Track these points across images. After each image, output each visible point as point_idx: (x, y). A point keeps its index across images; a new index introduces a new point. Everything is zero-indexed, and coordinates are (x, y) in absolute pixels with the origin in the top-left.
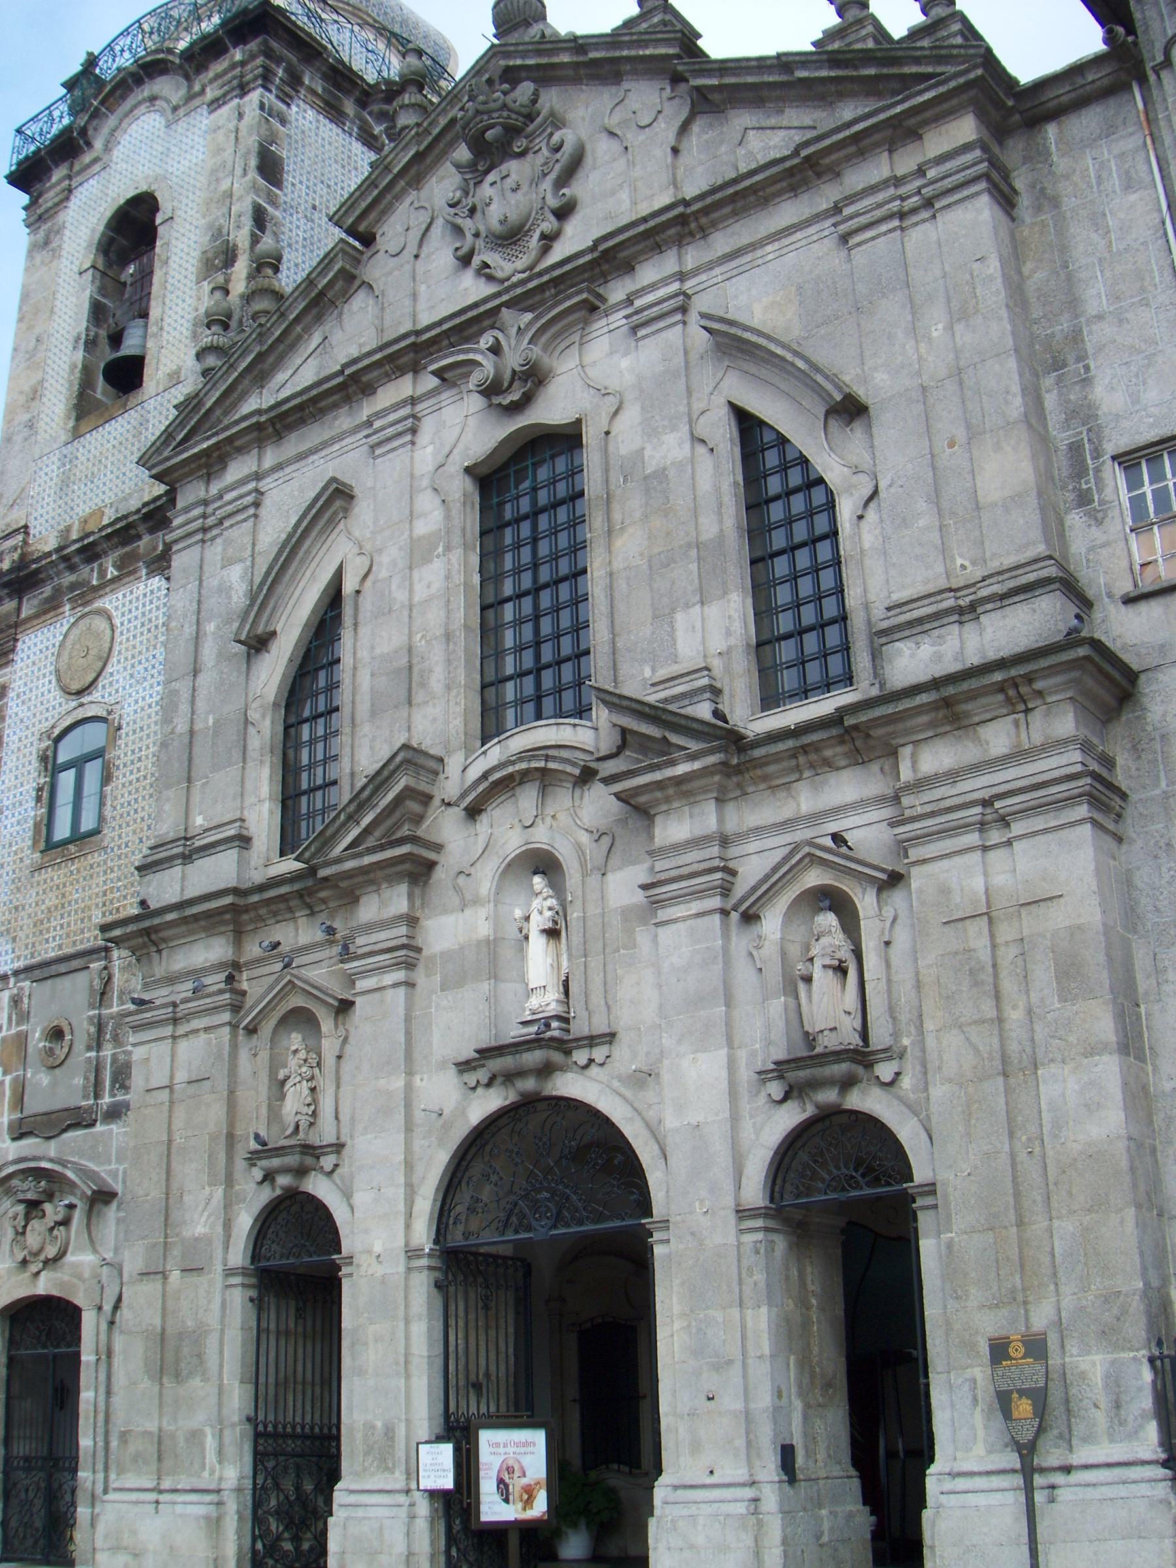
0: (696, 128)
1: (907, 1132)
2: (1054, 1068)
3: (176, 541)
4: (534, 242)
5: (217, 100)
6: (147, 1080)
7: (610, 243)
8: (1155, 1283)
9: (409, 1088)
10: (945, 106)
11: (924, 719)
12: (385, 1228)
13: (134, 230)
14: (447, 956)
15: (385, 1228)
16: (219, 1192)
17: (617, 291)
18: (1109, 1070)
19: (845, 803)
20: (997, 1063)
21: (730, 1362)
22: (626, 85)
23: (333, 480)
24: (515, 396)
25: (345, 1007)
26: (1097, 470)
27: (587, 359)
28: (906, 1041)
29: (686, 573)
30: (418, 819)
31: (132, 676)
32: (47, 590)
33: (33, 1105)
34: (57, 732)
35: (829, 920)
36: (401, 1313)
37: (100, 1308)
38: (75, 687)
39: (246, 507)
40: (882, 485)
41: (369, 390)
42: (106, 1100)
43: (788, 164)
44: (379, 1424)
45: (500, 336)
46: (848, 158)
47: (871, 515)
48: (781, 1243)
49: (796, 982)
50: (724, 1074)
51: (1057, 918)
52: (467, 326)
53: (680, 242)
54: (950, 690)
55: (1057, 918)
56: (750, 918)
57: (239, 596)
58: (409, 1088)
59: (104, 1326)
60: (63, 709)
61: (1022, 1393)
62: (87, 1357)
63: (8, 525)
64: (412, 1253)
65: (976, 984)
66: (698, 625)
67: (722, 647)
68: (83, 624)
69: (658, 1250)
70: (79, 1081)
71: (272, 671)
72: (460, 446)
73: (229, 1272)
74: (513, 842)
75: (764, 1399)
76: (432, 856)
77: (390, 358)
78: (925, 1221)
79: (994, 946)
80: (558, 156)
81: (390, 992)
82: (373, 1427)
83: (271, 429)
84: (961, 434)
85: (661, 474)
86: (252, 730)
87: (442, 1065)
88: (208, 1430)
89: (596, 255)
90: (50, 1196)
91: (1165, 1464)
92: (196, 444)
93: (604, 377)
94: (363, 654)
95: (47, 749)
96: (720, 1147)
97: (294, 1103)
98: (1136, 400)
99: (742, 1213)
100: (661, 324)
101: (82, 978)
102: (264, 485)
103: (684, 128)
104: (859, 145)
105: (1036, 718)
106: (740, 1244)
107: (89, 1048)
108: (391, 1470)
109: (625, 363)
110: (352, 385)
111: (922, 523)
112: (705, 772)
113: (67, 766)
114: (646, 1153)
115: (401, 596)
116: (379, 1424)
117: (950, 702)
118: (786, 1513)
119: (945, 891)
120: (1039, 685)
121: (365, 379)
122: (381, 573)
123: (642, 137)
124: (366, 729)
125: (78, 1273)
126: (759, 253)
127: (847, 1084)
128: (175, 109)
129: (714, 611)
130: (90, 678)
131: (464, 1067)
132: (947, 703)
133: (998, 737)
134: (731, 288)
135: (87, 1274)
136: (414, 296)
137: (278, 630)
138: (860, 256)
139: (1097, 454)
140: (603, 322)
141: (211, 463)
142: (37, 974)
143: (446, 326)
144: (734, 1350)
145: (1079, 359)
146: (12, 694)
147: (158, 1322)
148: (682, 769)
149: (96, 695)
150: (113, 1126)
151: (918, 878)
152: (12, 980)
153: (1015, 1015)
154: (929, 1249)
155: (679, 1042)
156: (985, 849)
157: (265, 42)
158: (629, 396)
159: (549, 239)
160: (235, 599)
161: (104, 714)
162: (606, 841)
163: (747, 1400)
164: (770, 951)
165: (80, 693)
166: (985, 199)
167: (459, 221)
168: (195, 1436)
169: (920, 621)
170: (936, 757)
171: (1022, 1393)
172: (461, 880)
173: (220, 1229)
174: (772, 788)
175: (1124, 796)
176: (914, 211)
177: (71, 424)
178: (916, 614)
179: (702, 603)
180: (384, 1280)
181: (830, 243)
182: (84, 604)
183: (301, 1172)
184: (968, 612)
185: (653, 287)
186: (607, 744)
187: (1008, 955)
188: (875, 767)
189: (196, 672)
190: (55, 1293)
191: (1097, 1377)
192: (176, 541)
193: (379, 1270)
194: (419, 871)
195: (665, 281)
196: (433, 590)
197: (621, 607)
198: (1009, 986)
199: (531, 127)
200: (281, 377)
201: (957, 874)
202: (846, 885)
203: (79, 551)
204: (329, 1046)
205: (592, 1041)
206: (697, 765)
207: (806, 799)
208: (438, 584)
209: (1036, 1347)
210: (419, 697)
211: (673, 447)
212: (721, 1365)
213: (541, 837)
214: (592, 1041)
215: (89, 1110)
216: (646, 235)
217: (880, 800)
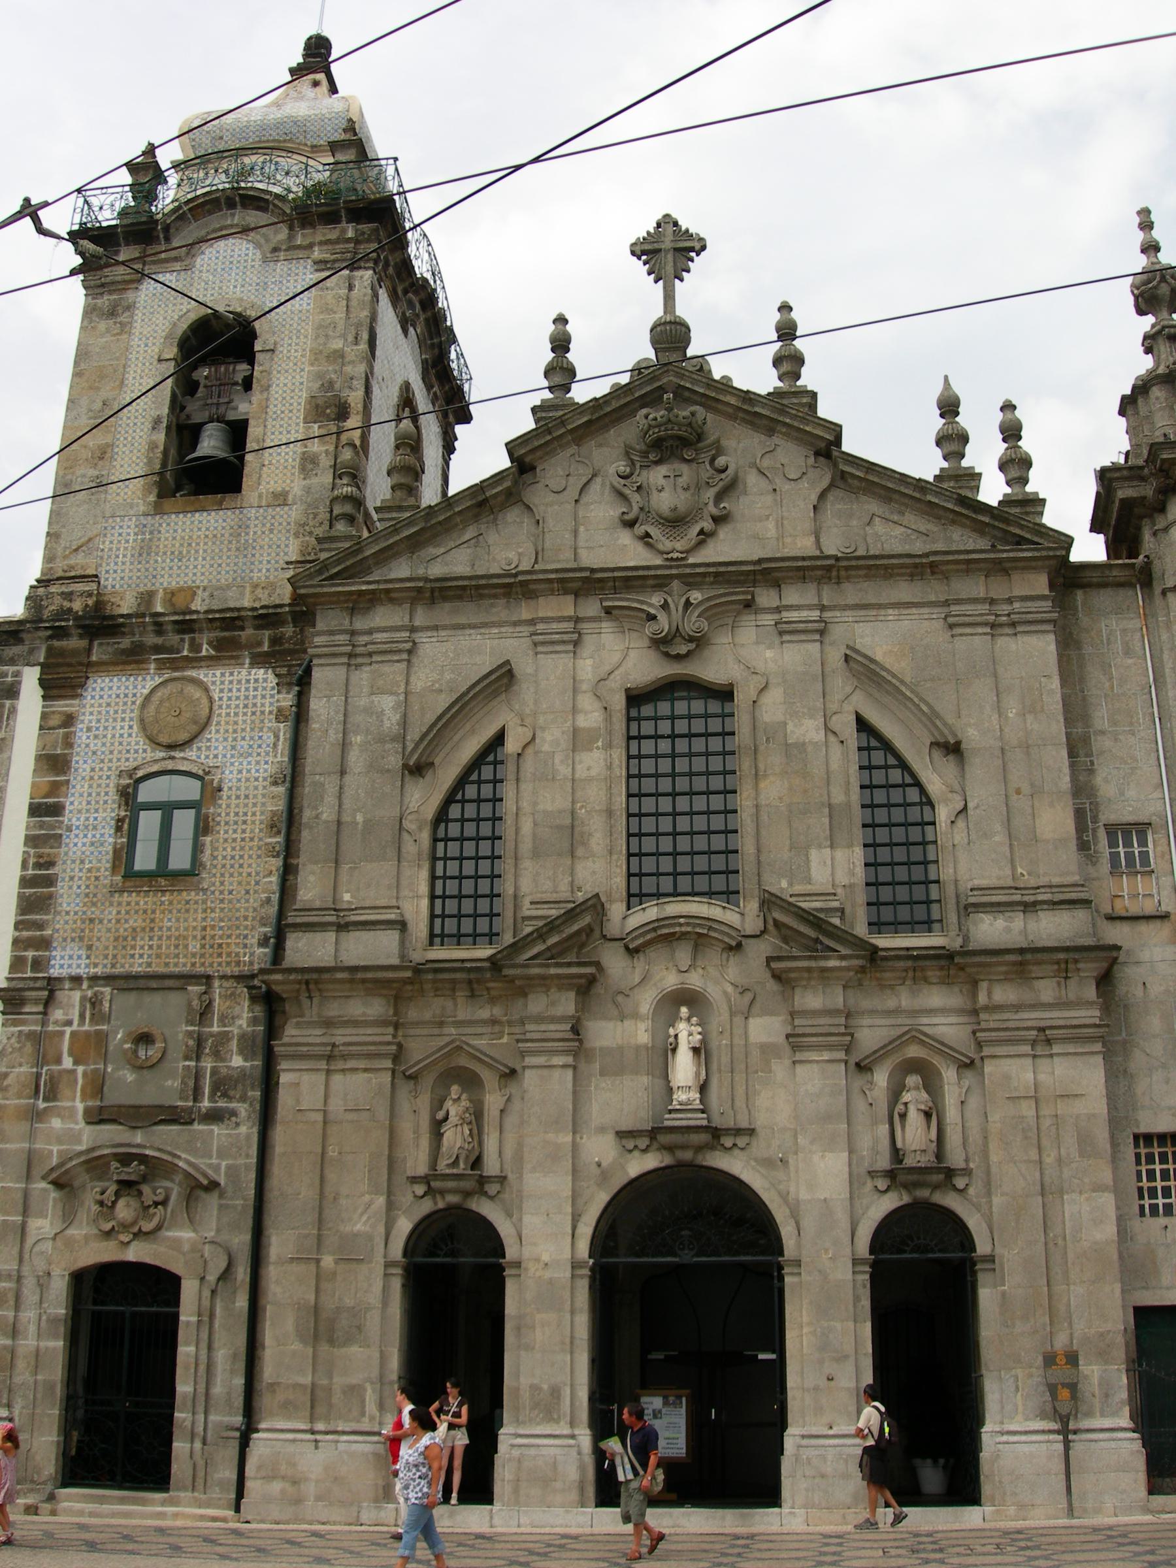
0: (830, 497)
1: (973, 1222)
2: (1074, 1196)
3: (319, 656)
6: (298, 1101)
7: (773, 565)
9: (575, 1147)
10: (1034, 564)
11: (1004, 969)
12: (547, 1246)
15: (547, 1246)
16: (381, 1200)
17: (766, 597)
20: (1038, 1188)
21: (846, 1357)
22: (776, 439)
23: (508, 662)
24: (683, 649)
25: (511, 1074)
26: (1094, 830)
27: (737, 640)
28: (972, 1165)
29: (820, 823)
30: (583, 945)
31: (233, 748)
32: (125, 643)
33: (114, 1097)
34: (140, 773)
36: (567, 1307)
37: (202, 1279)
38: (164, 739)
39: (400, 651)
40: (970, 805)
42: (206, 1104)
43: (917, 561)
44: (545, 1387)
45: (670, 600)
46: (958, 571)
47: (961, 824)
49: (896, 1116)
50: (846, 1169)
51: (1079, 1107)
53: (819, 581)
54: (1029, 956)
55: (1079, 1107)
56: (863, 1068)
58: (575, 1147)
59: (207, 1293)
60: (149, 755)
61: (1064, 1385)
62: (187, 1316)
63: (72, 568)
64: (575, 1265)
65: (1026, 1138)
66: (829, 862)
67: (845, 881)
68: (170, 687)
72: (621, 670)
73: (388, 1265)
74: (670, 980)
77: (561, 581)
78: (981, 1277)
80: (723, 476)
81: (557, 1073)
82: (540, 1389)
83: (428, 595)
84: (1026, 789)
85: (801, 746)
86: (405, 835)
87: (602, 1130)
88: (368, 1386)
89: (757, 568)
90: (144, 1179)
92: (353, 584)
93: (749, 655)
94: (525, 805)
95: (128, 786)
97: (454, 1138)
98: (1122, 794)
99: (856, 1262)
100: (803, 637)
101: (175, 999)
102: (421, 637)
103: (822, 496)
104: (969, 566)
105: (1072, 983)
107: (187, 1058)
108: (557, 1421)
109: (769, 654)
110: (516, 588)
111: (997, 839)
112: (848, 969)
113: (150, 806)
114: (780, 1214)
115: (564, 770)
116: (545, 1387)
117: (1023, 961)
119: (1007, 1077)
120: (1080, 965)
121: (532, 587)
123: (787, 486)
124: (527, 864)
125: (185, 1245)
126: (883, 612)
128: (275, 250)
129: (840, 854)
130: (183, 736)
131: (621, 1135)
133: (1046, 990)
134: (859, 628)
135: (186, 1247)
136: (576, 532)
137: (437, 761)
138: (961, 644)
139: (1095, 820)
140: (753, 617)
142: (121, 983)
143: (616, 574)
144: (849, 1348)
145: (1087, 755)
147: (311, 1297)
148: (832, 963)
149: (191, 754)
150: (215, 1128)
151: (989, 1067)
152: (85, 985)
153: (1049, 1159)
155: (812, 1142)
156: (1035, 1056)
157: (376, 230)
158: (773, 680)
159: (705, 536)
160: (387, 724)
161: (201, 773)
162: (748, 996)
165: (171, 747)
167: (627, 491)
168: (354, 1391)
169: (999, 904)
170: (1004, 994)
171: (1064, 1385)
172: (620, 998)
173: (381, 1229)
174: (882, 987)
176: (1001, 625)
177: (152, 498)
178: (994, 899)
179: (832, 847)
180: (551, 1281)
182: (176, 669)
184: (1029, 907)
187: (1046, 1123)
188: (956, 989)
189: (343, 773)
190: (148, 1260)
191: (1095, 1380)
192: (319, 656)
193: (548, 1274)
194: (586, 988)
196: (593, 773)
197: (763, 832)
198: (1045, 1142)
199: (700, 445)
200: (432, 551)
201: (1013, 1071)
202: (936, 1060)
203: (176, 622)
204: (493, 1101)
205: (738, 1132)
206: (844, 964)
207: (904, 999)
209: (1072, 1359)
210: (580, 852)
211: (809, 730)
212: (842, 1358)
213: (695, 980)
215: (189, 1110)
216: (799, 569)
217: (960, 1012)
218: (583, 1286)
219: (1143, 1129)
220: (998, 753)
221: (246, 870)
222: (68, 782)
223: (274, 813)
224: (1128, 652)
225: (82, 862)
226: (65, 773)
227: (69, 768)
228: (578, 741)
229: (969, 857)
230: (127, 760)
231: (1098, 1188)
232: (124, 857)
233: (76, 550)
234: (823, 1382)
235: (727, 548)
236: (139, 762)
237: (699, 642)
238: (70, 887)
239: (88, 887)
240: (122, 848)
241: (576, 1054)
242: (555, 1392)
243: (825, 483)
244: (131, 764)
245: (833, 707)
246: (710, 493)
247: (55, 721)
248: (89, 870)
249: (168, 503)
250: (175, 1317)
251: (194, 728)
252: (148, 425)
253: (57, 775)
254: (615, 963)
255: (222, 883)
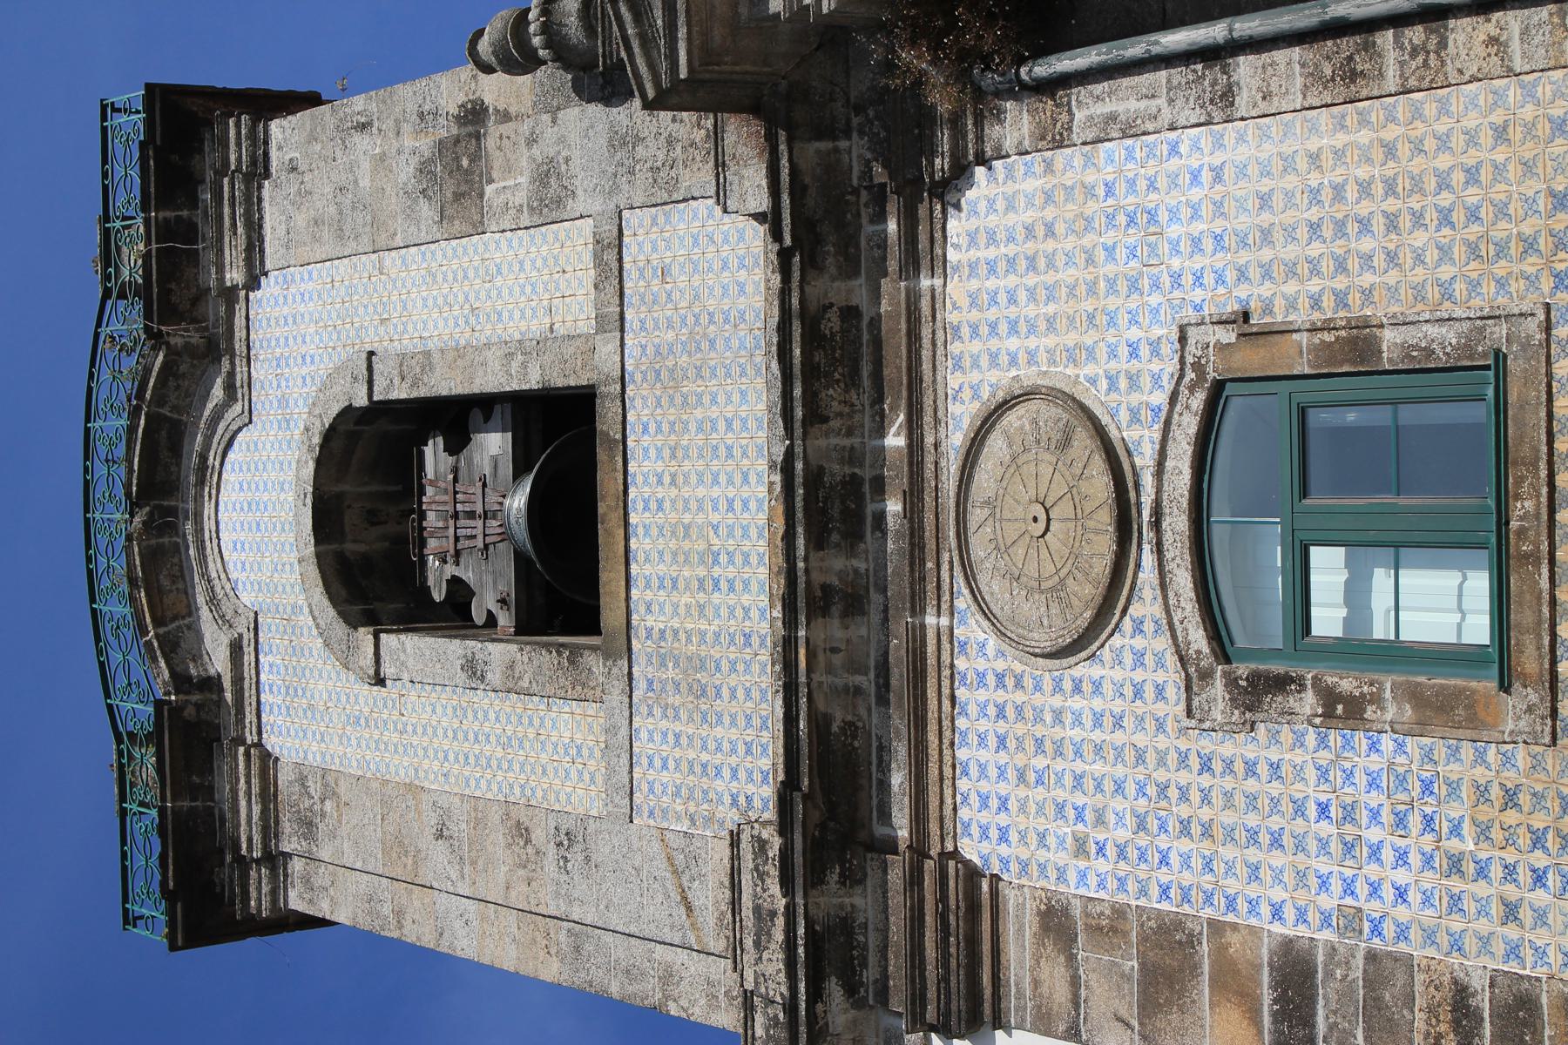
5: (250, 248)
34: (1198, 639)
95: (1231, 682)
130: (1100, 486)
146: (1071, 888)
149: (1142, 443)
221: (1488, 153)
222: (1216, 927)
223: (1315, 77)
225: (1455, 865)
226: (1192, 941)
227: (1178, 923)
230: (1160, 691)
232: (1445, 691)
233: (689, 909)
236: (1163, 643)
238: (1541, 917)
239: (1538, 841)
240: (1415, 696)
244: (1171, 677)
248: (1483, 833)
249: (611, 616)
251: (1083, 440)
252: (481, 699)
253: (1195, 968)
255: (1529, 245)
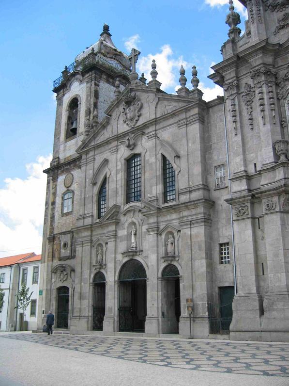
0: (159, 103)
1: (179, 268)
4: (135, 121)
8: (210, 292)
12: (111, 278)
13: (74, 103)
14: (121, 237)
15: (111, 278)
16: (89, 271)
18: (204, 261)
19: (173, 218)
25: (107, 243)
30: (117, 215)
33: (62, 255)
35: (170, 236)
38: (67, 186)
41: (111, 143)
47: (180, 174)
48: (163, 283)
52: (124, 135)
56: (161, 235)
57: (91, 176)
62: (70, 294)
69: (147, 283)
70: (69, 252)
71: (96, 189)
73: (90, 284)
74: (130, 220)
75: (160, 305)
76: (118, 221)
78: (181, 281)
79: (191, 242)
85: (151, 164)
87: (120, 253)
91: (208, 318)
93: (145, 145)
94: (110, 188)
96: (155, 268)
98: (218, 158)
103: (157, 104)
106: (157, 283)
110: (107, 142)
112: (155, 213)
118: (162, 322)
119: (185, 233)
120: (198, 204)
122: (112, 175)
127: (172, 261)
131: (123, 254)
132: (187, 206)
141: (87, 152)
148: (152, 212)
149: (70, 188)
154: (181, 285)
163: (158, 305)
164: (163, 240)
166: (198, 123)
170: (186, 213)
175: (212, 220)
181: (177, 128)
183: (100, 268)
185: (151, 132)
186: (143, 206)
189: (85, 187)
193: (110, 284)
194: (117, 223)
195: (153, 131)
200: (97, 138)
201: (186, 231)
204: (104, 249)
205: (140, 251)
207: (168, 217)
208: (120, 178)
209: (192, 300)
211: (153, 160)
213: (134, 220)
214: (140, 251)
218: (116, 286)
219: (221, 242)
220: (187, 155)
224: (221, 121)
228: (117, 173)
229: (182, 183)
231: (202, 258)
234: (152, 305)
235: (141, 122)
237: (135, 145)
241: (115, 238)
242: (111, 308)
243: (157, 101)
245: (157, 153)
246: (136, 111)
247: (54, 187)
250: (69, 295)
254: (123, 219)
